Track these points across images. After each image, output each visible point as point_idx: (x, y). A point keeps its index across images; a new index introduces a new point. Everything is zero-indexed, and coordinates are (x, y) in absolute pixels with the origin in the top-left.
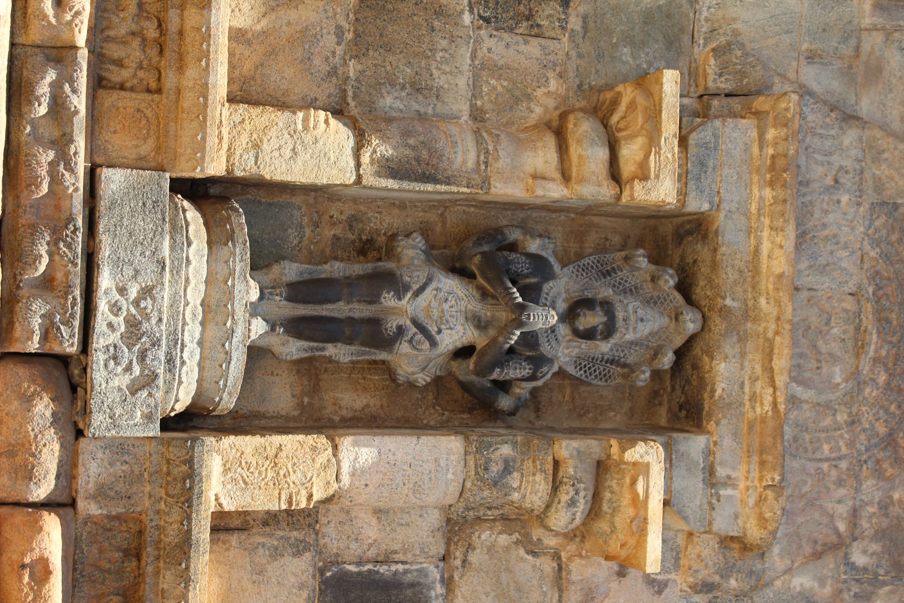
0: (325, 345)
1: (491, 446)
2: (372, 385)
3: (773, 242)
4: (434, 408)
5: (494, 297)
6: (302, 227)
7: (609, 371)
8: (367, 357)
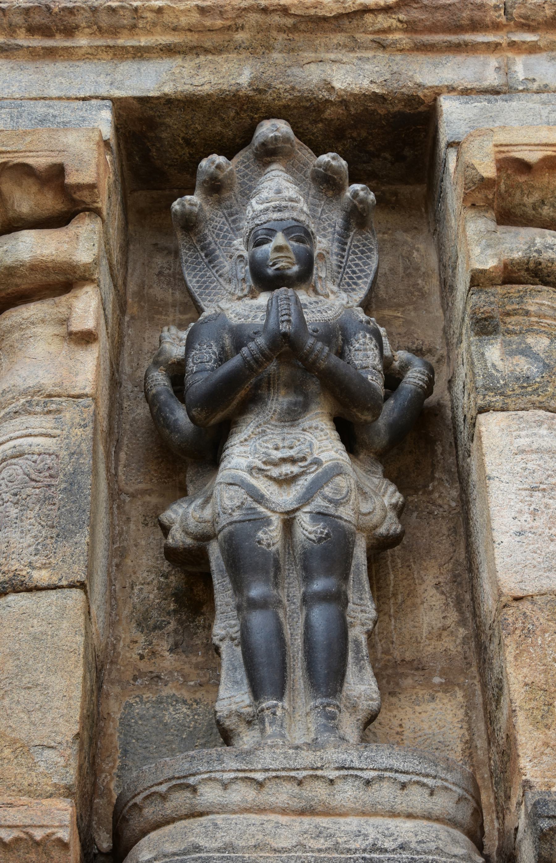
0: (350, 639)
1: (491, 375)
2: (405, 583)
3: (154, 24)
4: (431, 493)
5: (257, 386)
6: (160, 701)
7: (356, 246)
8: (365, 576)
